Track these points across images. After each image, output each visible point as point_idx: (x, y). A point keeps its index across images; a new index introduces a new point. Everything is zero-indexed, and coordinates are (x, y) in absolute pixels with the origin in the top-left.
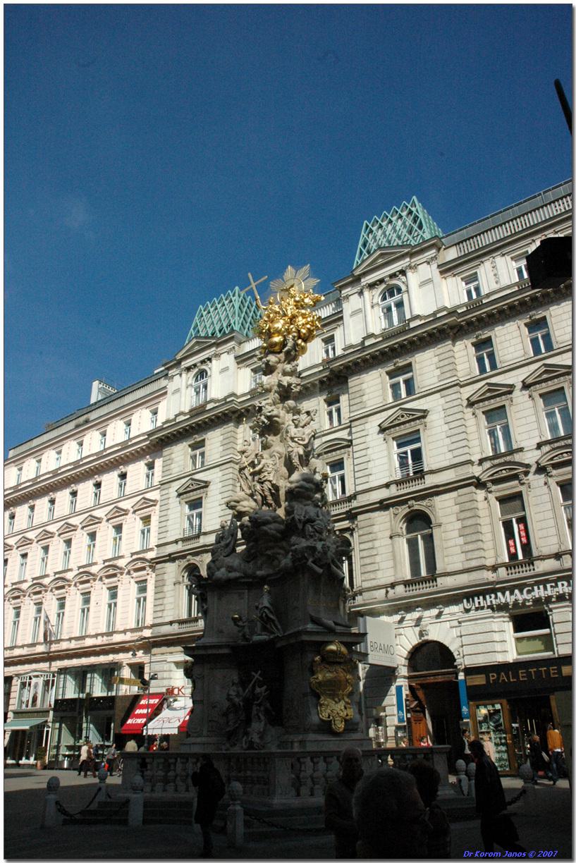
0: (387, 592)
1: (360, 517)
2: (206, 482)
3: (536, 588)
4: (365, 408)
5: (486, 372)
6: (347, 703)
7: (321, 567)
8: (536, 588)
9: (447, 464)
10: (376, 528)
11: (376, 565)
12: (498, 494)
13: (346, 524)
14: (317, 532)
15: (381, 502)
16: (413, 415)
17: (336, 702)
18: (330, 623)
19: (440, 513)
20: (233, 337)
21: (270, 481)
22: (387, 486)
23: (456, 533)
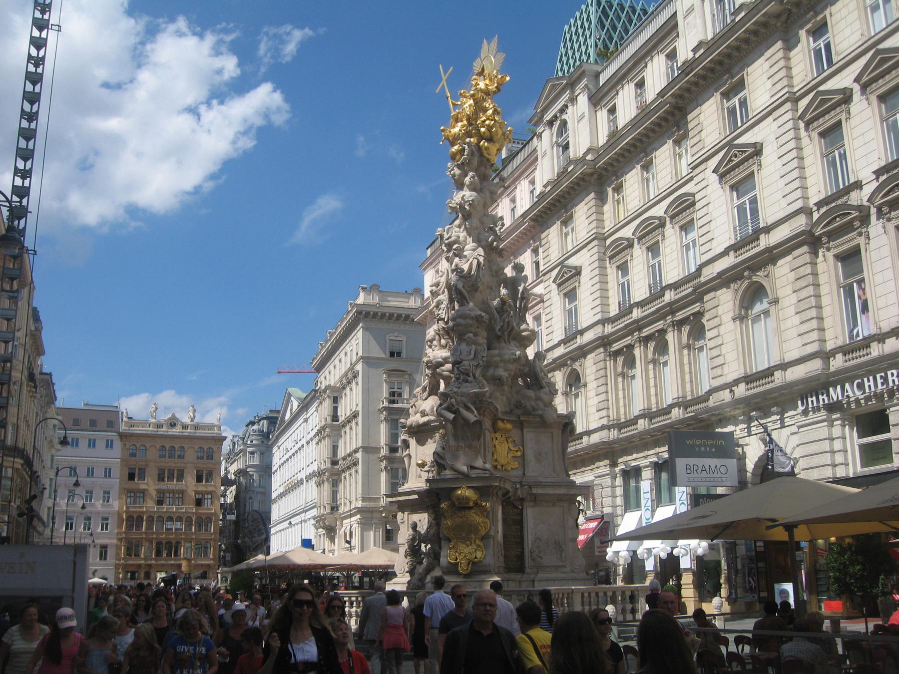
0: (731, 391)
1: (706, 298)
2: (575, 268)
3: (865, 379)
4: (703, 148)
5: (824, 71)
6: (478, 546)
7: (454, 412)
8: (865, 379)
9: (781, 215)
10: (720, 310)
11: (722, 357)
12: (836, 251)
13: (696, 308)
14: (463, 373)
15: (720, 274)
16: (745, 152)
17: (468, 546)
18: (465, 469)
19: (779, 283)
20: (584, 72)
21: (443, 319)
22: (725, 253)
23: (792, 310)
